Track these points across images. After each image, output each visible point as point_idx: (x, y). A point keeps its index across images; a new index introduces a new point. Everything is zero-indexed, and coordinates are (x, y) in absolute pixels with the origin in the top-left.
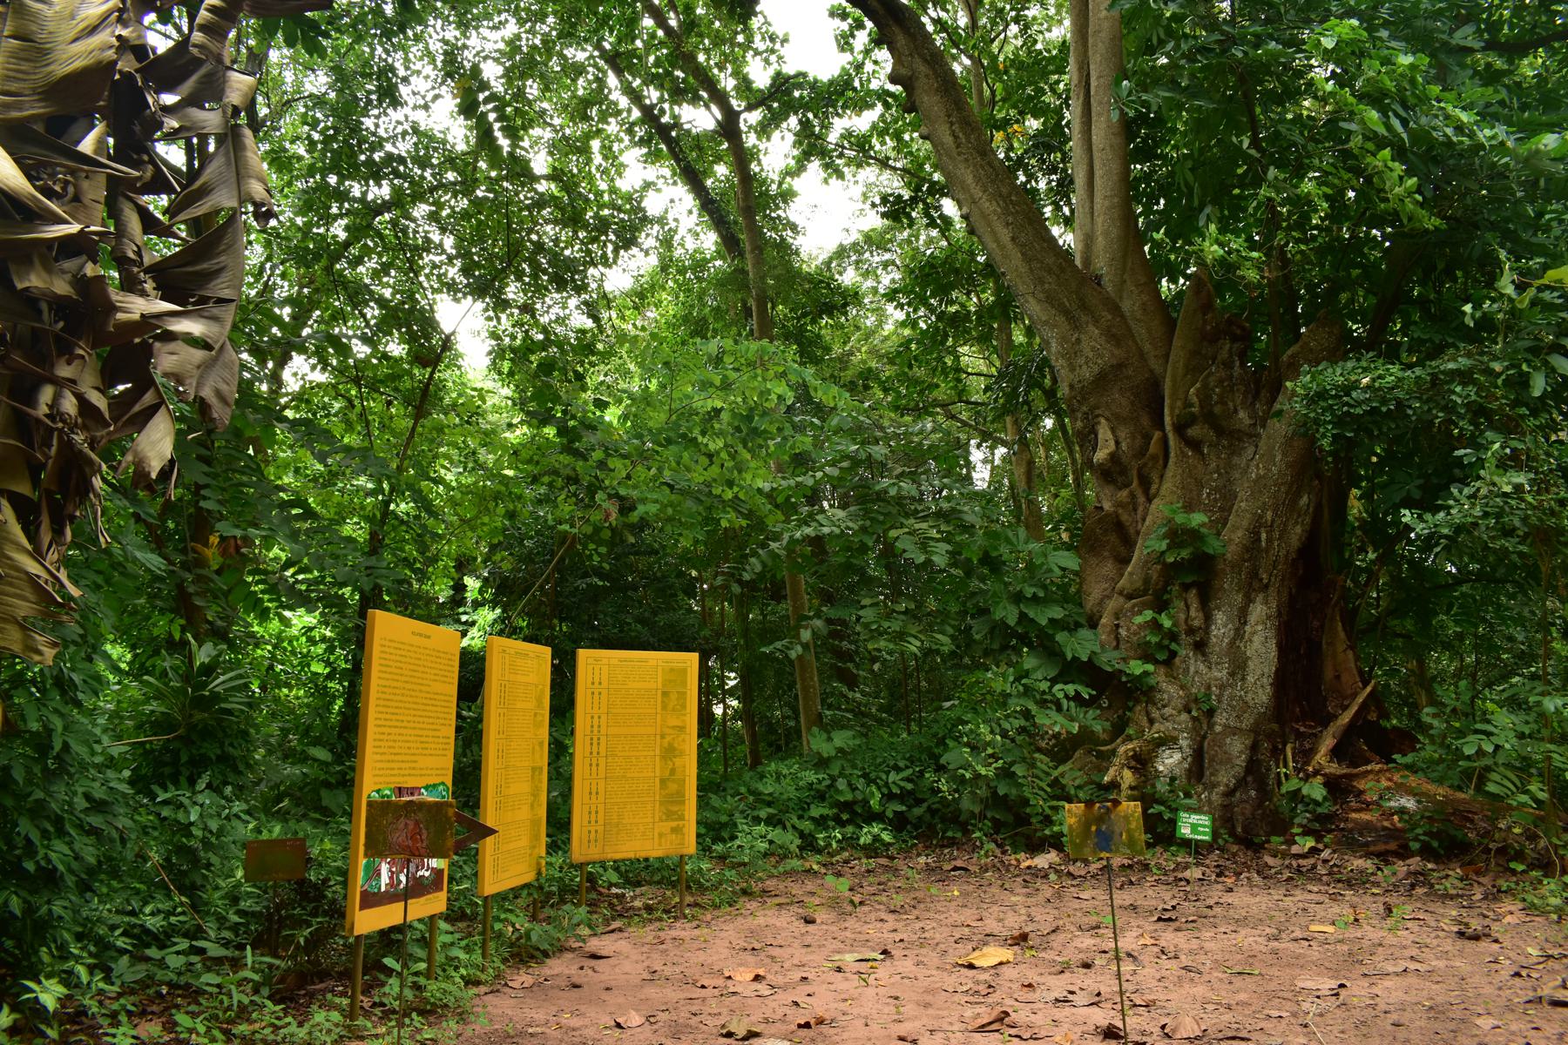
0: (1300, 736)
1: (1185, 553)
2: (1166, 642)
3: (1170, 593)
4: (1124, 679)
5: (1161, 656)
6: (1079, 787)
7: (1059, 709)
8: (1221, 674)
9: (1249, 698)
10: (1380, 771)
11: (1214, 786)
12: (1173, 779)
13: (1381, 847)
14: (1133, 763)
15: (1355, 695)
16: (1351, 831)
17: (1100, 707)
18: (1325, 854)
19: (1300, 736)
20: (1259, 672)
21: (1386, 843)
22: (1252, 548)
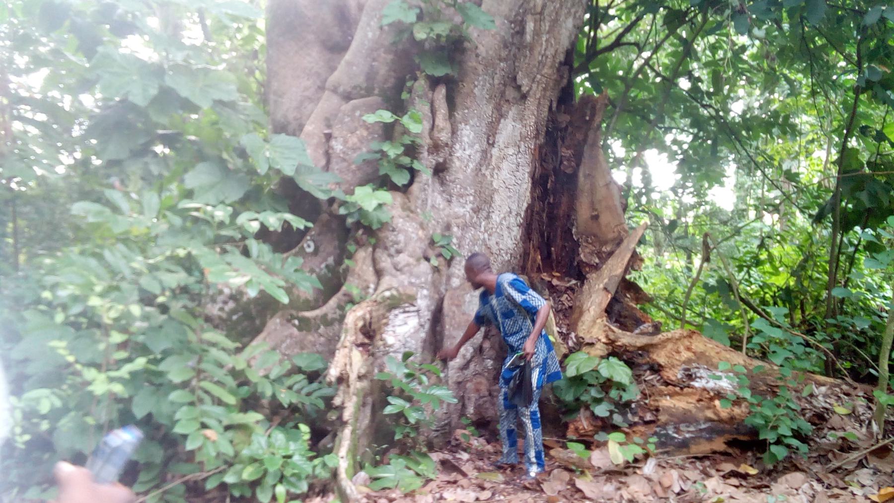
1: (442, 29)
2: (406, 160)
3: (410, 91)
4: (342, 211)
5: (400, 179)
6: (278, 380)
7: (246, 253)
8: (463, 209)
9: (492, 243)
12: (407, 356)
13: (704, 447)
16: (664, 426)
17: (302, 253)
21: (710, 440)
22: (516, 42)
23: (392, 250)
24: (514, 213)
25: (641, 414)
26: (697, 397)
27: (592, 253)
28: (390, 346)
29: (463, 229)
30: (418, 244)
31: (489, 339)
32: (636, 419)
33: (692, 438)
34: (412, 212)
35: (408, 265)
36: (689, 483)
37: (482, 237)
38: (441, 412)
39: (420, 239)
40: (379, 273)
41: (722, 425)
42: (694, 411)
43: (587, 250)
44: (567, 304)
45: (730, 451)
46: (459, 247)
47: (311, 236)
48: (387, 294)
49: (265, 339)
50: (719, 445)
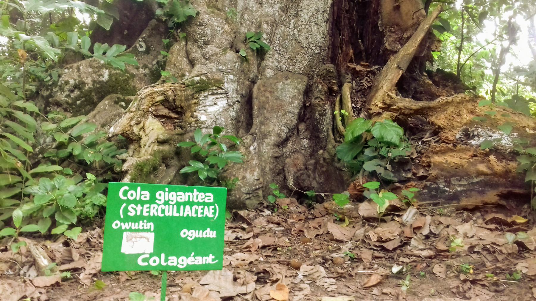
0: (356, 74)
9: (302, 38)
10: (461, 102)
11: (265, 136)
12: (217, 130)
14: (164, 111)
15: (416, 25)
18: (409, 216)
19: (356, 74)
20: (314, 8)
21: (482, 193)
23: (201, 42)
24: (321, 11)
25: (414, 171)
26: (471, 153)
27: (394, 41)
28: (203, 123)
29: (272, 26)
30: (225, 36)
31: (305, 122)
32: (410, 175)
33: (463, 190)
34: (219, 10)
35: (216, 54)
36: (442, 227)
37: (292, 33)
38: (252, 179)
39: (225, 32)
40: (192, 63)
41: (496, 179)
42: (466, 165)
43: (391, 39)
44: (366, 84)
45: (504, 203)
46: (271, 42)
47: (143, 38)
48: (197, 79)
49: (94, 117)
50: (492, 196)
